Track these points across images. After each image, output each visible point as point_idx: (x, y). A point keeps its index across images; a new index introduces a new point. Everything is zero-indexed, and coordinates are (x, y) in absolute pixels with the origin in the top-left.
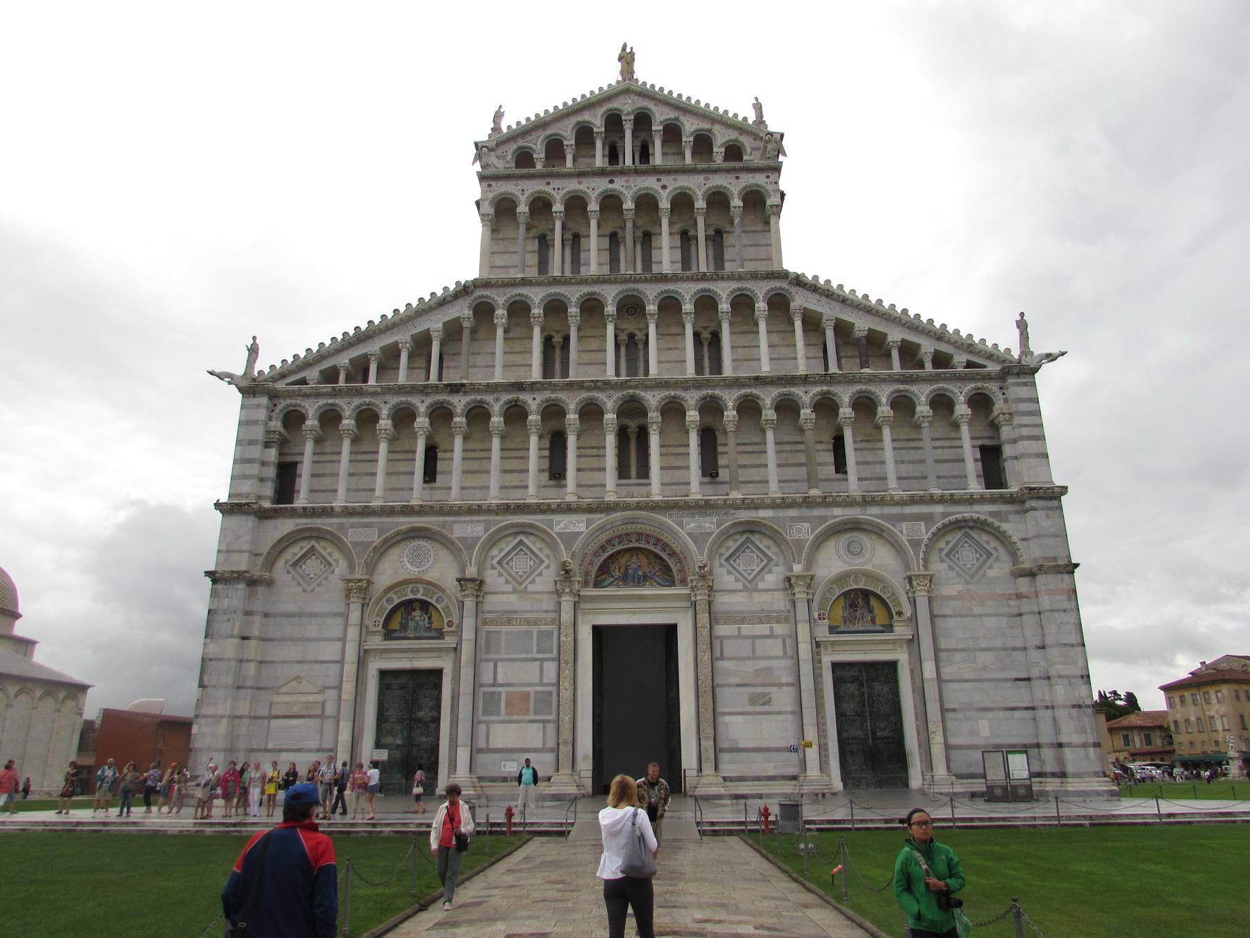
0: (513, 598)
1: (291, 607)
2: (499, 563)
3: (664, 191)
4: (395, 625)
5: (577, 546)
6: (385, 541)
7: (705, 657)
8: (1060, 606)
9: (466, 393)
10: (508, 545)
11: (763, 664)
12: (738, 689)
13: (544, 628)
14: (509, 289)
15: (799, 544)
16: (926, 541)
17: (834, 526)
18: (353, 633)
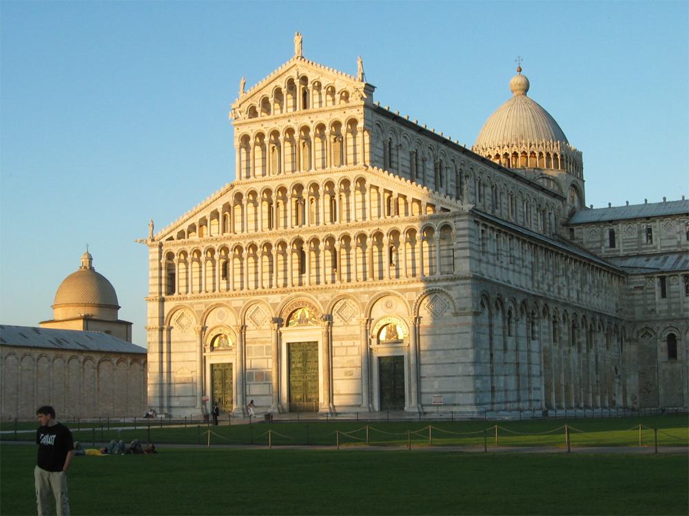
0: (256, 332)
1: (178, 339)
2: (251, 317)
3: (311, 121)
4: (216, 344)
5: (278, 309)
6: (207, 310)
7: (326, 355)
8: (465, 331)
9: (233, 240)
10: (252, 309)
11: (351, 358)
12: (341, 369)
13: (268, 345)
14: (246, 186)
15: (363, 304)
16: (416, 301)
17: (379, 295)
18: (198, 349)
